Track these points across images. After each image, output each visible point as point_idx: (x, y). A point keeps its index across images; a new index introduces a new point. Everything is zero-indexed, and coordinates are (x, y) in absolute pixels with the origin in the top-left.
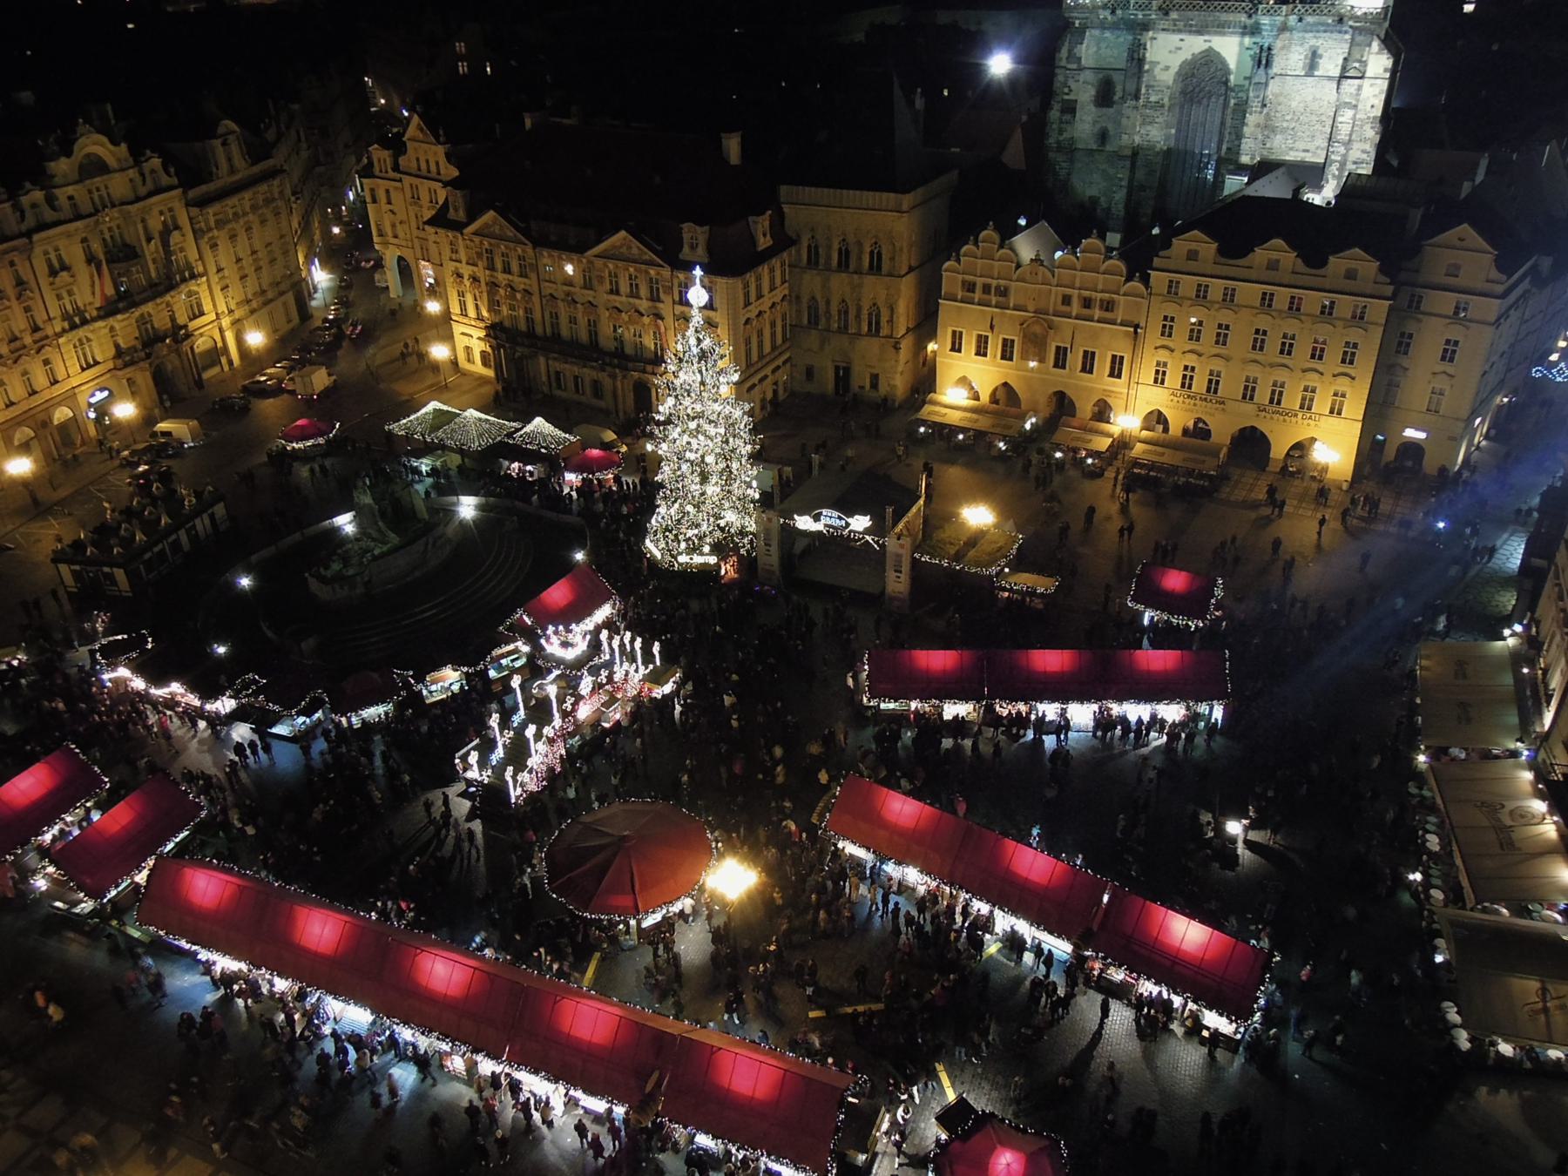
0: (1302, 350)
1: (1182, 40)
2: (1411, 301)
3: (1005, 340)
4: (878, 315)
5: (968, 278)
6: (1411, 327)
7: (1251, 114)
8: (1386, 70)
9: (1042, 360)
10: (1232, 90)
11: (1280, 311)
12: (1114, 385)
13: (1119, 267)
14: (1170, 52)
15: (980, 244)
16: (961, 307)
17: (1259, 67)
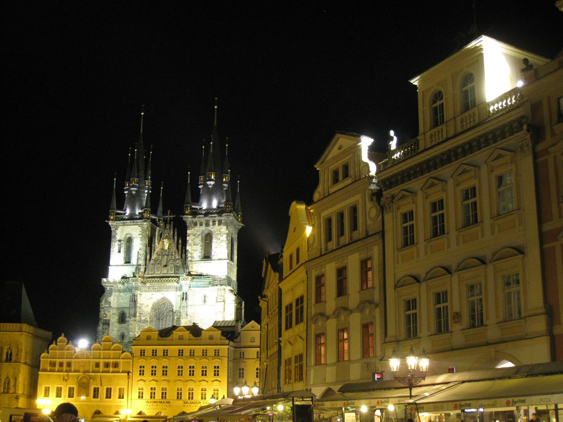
0: (198, 372)
1: (152, 294)
2: (240, 355)
3: (70, 389)
4: (9, 383)
5: (52, 360)
6: (242, 366)
7: (182, 319)
8: (233, 301)
9: (87, 395)
10: (175, 313)
11: (187, 357)
12: (121, 402)
13: (119, 346)
14: (148, 299)
15: (58, 343)
16: (49, 375)
17: (183, 300)
